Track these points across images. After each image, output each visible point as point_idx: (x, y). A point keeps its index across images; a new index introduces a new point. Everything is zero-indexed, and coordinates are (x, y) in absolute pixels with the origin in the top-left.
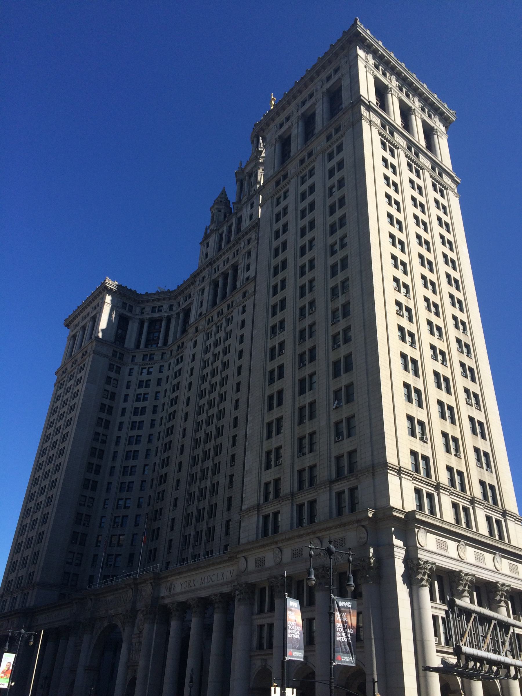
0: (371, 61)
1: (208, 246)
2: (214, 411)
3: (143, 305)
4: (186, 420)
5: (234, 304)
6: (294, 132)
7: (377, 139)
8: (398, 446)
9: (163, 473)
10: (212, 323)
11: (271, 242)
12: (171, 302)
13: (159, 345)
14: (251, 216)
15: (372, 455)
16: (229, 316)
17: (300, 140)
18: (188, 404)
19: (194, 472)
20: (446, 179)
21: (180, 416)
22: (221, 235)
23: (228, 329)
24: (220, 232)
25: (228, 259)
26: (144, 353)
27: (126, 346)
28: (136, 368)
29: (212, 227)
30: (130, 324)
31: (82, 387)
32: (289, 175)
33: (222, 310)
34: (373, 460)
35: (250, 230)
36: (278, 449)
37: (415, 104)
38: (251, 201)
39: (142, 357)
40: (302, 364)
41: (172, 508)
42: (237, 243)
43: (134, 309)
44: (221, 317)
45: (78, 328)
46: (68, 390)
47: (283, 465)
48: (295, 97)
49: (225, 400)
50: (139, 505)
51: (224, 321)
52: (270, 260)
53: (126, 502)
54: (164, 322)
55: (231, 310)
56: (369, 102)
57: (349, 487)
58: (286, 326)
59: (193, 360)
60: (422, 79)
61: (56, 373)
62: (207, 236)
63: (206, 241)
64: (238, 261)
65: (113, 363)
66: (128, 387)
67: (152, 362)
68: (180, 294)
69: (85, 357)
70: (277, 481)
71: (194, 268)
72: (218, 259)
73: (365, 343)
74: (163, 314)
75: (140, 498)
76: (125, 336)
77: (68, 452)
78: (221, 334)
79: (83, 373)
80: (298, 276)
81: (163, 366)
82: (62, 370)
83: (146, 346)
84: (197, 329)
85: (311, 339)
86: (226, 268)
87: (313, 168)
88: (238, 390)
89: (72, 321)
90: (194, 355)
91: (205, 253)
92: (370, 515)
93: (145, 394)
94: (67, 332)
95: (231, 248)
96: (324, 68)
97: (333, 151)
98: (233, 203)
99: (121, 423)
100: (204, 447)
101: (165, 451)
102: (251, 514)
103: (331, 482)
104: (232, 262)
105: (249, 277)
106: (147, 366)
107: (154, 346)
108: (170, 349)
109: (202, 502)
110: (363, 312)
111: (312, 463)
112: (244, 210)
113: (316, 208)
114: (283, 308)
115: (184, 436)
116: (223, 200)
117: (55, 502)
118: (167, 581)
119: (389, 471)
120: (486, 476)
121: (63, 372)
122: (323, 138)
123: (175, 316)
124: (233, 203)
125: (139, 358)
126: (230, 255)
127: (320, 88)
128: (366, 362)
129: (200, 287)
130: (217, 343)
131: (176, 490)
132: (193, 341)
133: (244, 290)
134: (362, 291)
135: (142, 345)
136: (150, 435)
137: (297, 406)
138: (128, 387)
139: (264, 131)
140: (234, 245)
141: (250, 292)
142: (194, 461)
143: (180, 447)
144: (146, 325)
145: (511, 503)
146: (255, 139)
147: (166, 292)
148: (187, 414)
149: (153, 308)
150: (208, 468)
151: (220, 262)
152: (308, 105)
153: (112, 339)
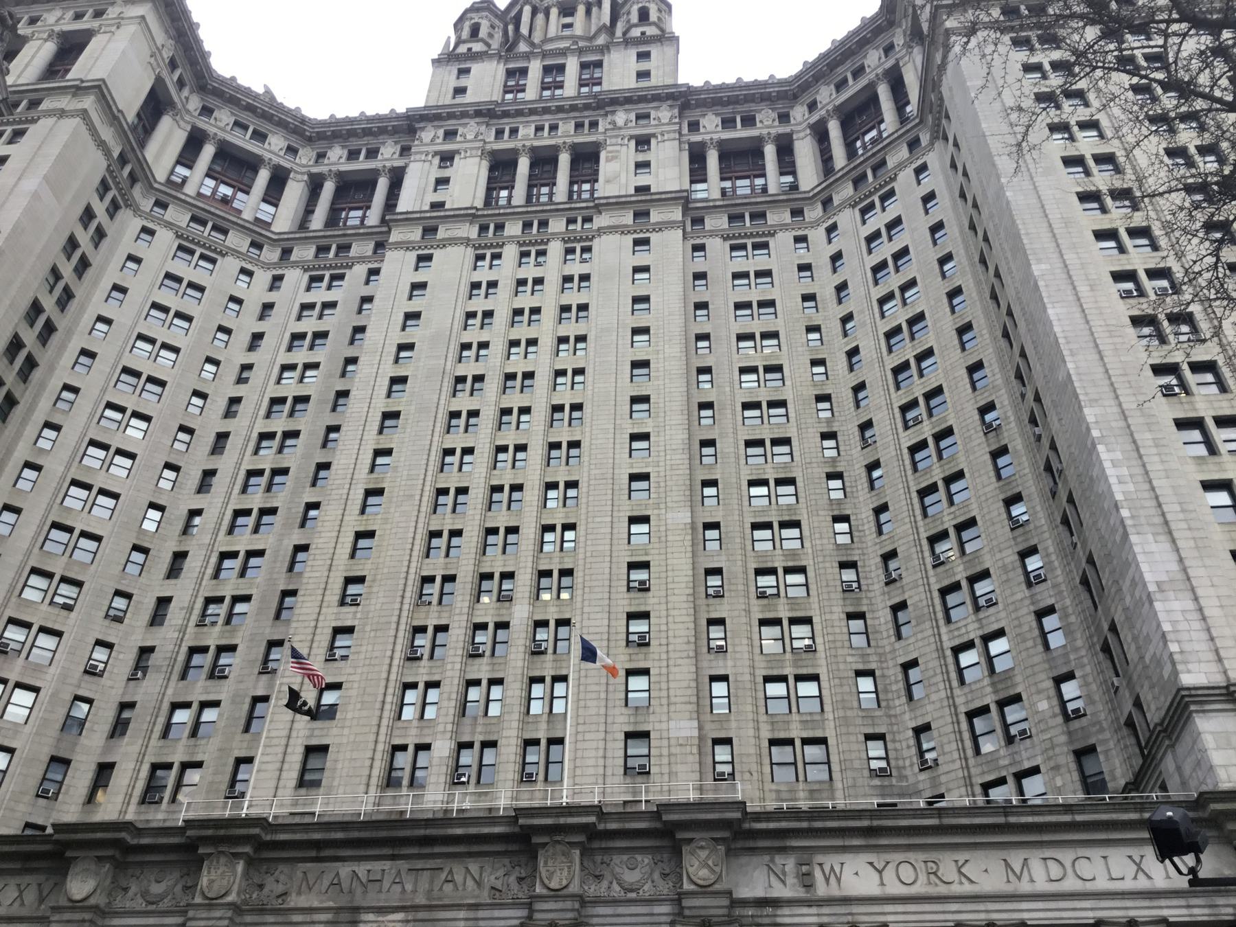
3: (212, 102)
24: (511, 66)
28: (165, 239)
30: (166, 122)
54: (263, 176)
91: (452, 82)
108: (287, 245)
109: (485, 660)
118: (783, 850)
123: (306, 177)
144: (208, 151)
153: (131, 116)
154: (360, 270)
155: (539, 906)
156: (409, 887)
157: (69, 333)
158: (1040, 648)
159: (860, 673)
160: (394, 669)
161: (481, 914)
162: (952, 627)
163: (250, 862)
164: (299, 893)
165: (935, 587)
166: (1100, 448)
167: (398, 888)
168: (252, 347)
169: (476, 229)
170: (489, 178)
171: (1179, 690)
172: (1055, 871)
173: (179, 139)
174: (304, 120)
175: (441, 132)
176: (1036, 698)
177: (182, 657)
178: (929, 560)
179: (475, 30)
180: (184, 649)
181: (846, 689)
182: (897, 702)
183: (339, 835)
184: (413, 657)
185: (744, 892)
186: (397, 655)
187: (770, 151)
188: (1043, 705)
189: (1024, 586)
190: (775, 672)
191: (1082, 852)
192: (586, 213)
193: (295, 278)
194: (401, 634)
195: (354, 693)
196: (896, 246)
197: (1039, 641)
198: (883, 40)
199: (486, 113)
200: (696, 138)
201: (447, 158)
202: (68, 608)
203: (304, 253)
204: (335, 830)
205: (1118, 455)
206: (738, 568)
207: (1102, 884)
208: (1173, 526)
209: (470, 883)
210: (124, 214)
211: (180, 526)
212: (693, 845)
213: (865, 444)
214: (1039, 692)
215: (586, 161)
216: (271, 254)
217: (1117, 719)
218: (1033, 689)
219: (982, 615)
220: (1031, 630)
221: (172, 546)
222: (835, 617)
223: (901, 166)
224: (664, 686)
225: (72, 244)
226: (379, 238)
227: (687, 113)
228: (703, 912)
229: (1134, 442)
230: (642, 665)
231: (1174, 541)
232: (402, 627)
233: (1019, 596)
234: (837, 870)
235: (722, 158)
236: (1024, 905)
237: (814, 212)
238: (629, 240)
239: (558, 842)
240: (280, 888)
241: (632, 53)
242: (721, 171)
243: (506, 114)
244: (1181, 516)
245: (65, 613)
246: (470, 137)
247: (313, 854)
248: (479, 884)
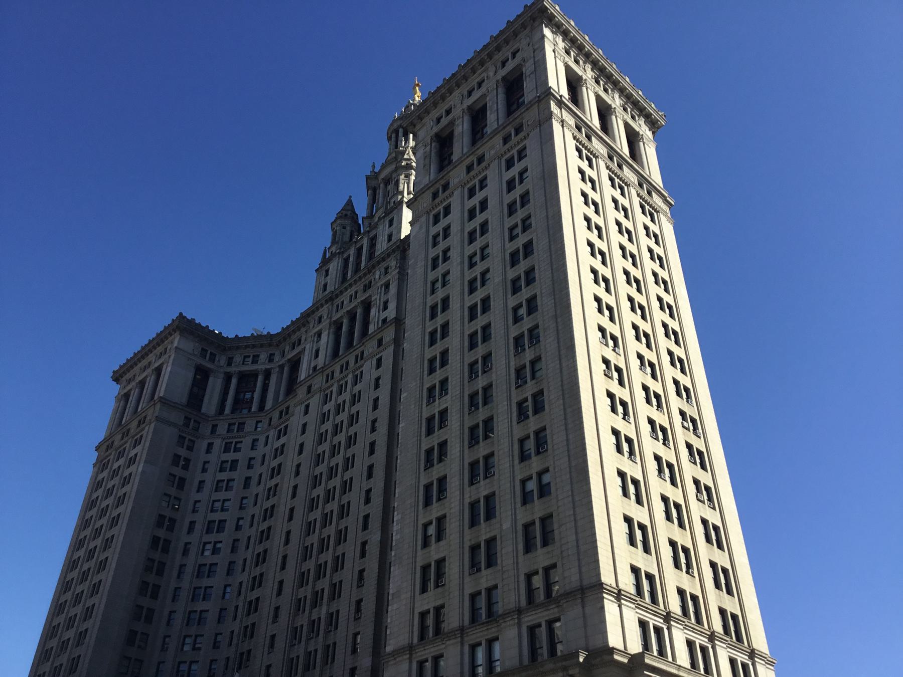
0: (561, 45)
1: (327, 275)
2: (334, 506)
4: (290, 518)
5: (365, 355)
6: (458, 130)
7: (571, 144)
8: (616, 560)
9: (253, 598)
10: (333, 381)
11: (426, 273)
13: (254, 409)
14: (390, 237)
15: (580, 572)
16: (358, 372)
17: (467, 140)
18: (294, 495)
19: (301, 595)
20: (657, 200)
21: (282, 511)
22: (346, 261)
23: (357, 389)
24: (345, 256)
25: (356, 293)
26: (232, 421)
27: (203, 410)
28: (218, 444)
29: (333, 249)
30: (211, 380)
31: (138, 469)
32: (451, 185)
33: (347, 363)
34: (581, 580)
35: (389, 255)
36: (440, 563)
37: (615, 101)
38: (391, 216)
39: (227, 426)
40: (473, 441)
41: (266, 649)
42: (370, 272)
43: (217, 359)
44: (345, 373)
45: (133, 384)
46: (115, 473)
47: (447, 587)
48: (458, 85)
49: (350, 490)
50: (216, 646)
51: (350, 378)
52: (425, 296)
53: (195, 640)
54: (260, 378)
55: (360, 363)
56: (561, 96)
57: (547, 618)
58: (450, 387)
59: (303, 432)
60: (623, 71)
61: (97, 449)
62: (325, 261)
63: (325, 268)
64: (370, 296)
65: (184, 435)
66: (204, 470)
67: (241, 434)
68: (285, 339)
69: (142, 426)
70: (438, 610)
71: (307, 303)
72: (341, 292)
73: (565, 414)
74: (262, 366)
75: (217, 635)
76: (203, 396)
77: (112, 565)
78: (346, 396)
79: (138, 449)
80: (466, 320)
81: (258, 440)
82: (106, 444)
83: (233, 411)
84: (310, 388)
85: (486, 407)
86: (353, 306)
87: (485, 178)
88: (370, 476)
89: (124, 373)
90: (305, 425)
92: (581, 660)
93: (229, 481)
94: (115, 389)
95: (360, 278)
96: (498, 49)
97: (513, 157)
98: (363, 218)
99: (192, 523)
100: (317, 559)
101: (257, 565)
102: (401, 658)
103: (519, 611)
104: (362, 297)
105: (386, 319)
107: (245, 411)
108: (269, 416)
109: (312, 641)
110: (561, 372)
111: (490, 584)
112: (380, 228)
113: (490, 229)
114: (444, 363)
115: (287, 542)
116: (348, 213)
117: (91, 639)
119: (605, 595)
120: (727, 601)
121: (108, 448)
122: (498, 140)
123: (277, 369)
124: (363, 218)
125: (222, 429)
126: (359, 287)
127: (493, 75)
128: (567, 440)
129: (316, 330)
130: (339, 409)
131: (274, 622)
132: (303, 406)
133: (379, 336)
134: (558, 343)
135: (227, 410)
136: (235, 541)
137: (467, 501)
138: (204, 470)
139: (415, 126)
140: (365, 275)
141: (388, 339)
142: (303, 579)
143: (280, 558)
144: (234, 381)
145: (759, 640)
146: (394, 135)
147: (265, 336)
148: (292, 510)
149: (245, 357)
150: (323, 590)
151: (345, 298)
152: (476, 95)
153: (184, 400)
192: (361, 349)
201: (319, 335)
211: (236, 594)
230: (358, 630)
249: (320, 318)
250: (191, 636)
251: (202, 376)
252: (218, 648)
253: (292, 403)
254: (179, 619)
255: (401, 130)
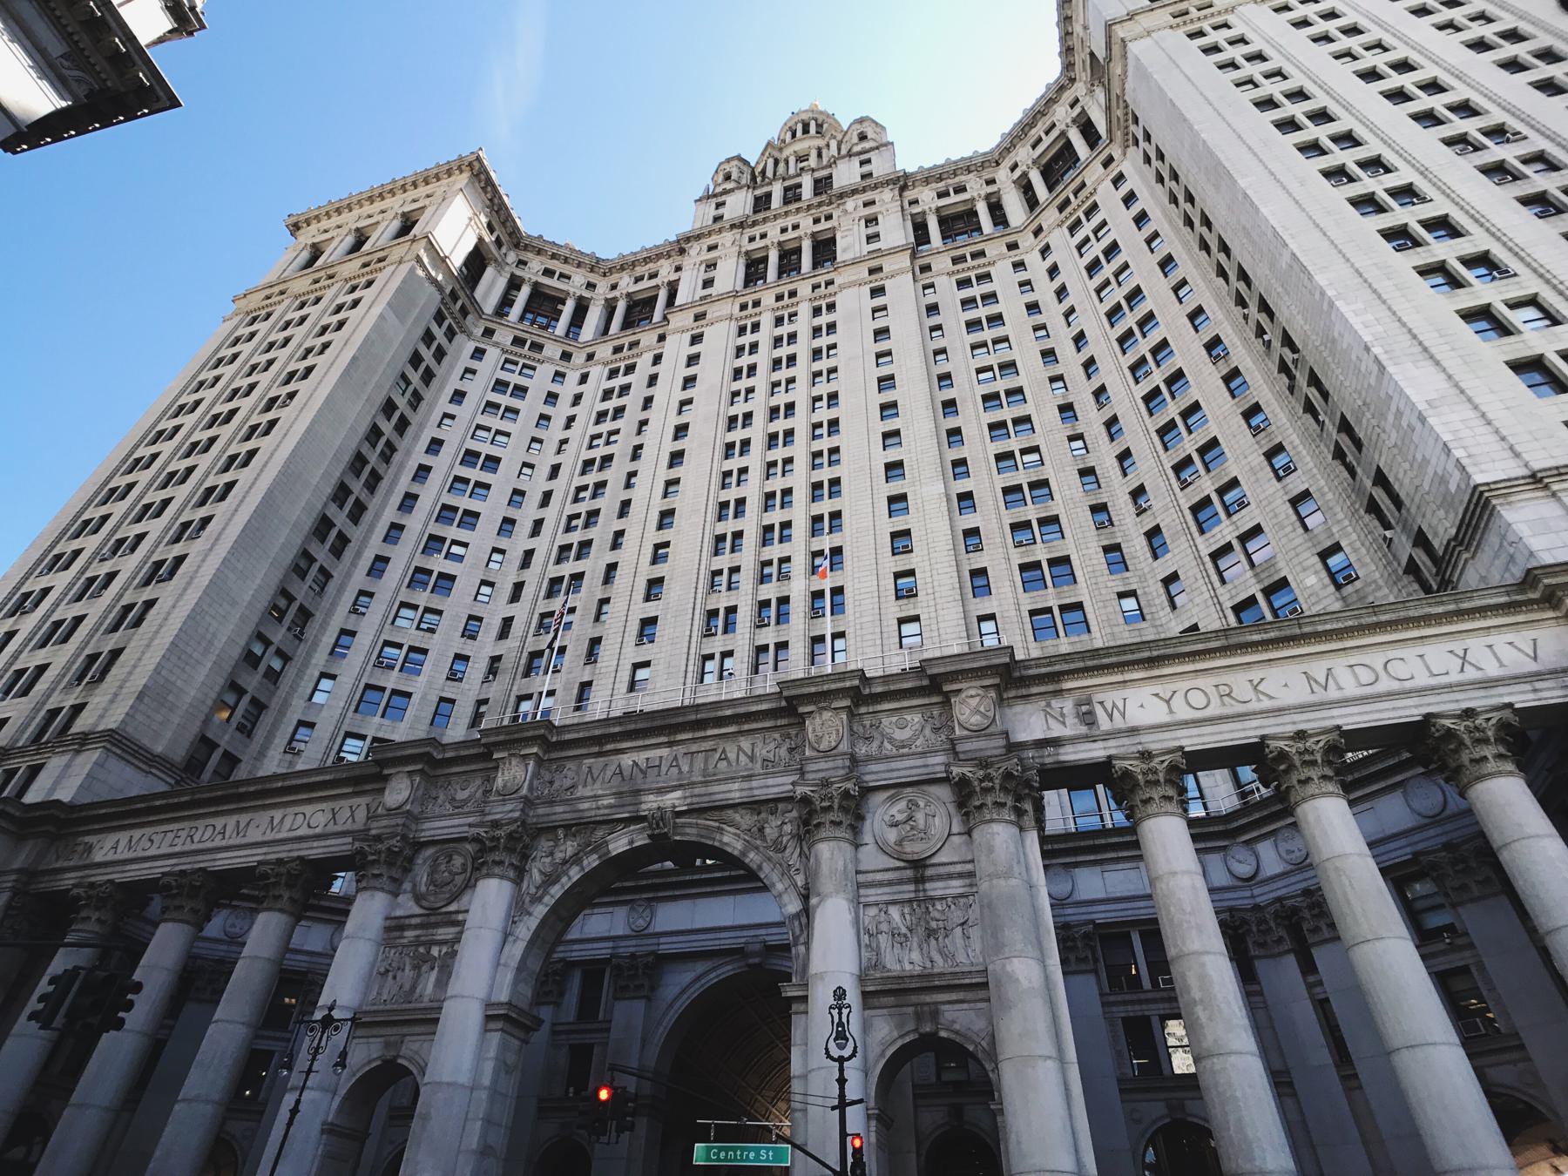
12: (593, 278)
24: (758, 192)
30: (490, 272)
42: (831, 203)
63: (714, 201)
67: (537, 356)
82: (267, 292)
91: (712, 212)
106: (522, 361)
108: (590, 350)
125: (504, 336)
131: (647, 599)
144: (525, 291)
146: (799, 128)
154: (648, 357)
155: (811, 767)
156: (685, 768)
157: (422, 426)
158: (1301, 530)
159: (1121, 595)
160: (693, 645)
161: (754, 784)
162: (1207, 535)
163: (540, 762)
164: (585, 785)
165: (1185, 506)
166: (1338, 303)
167: (675, 770)
168: (568, 427)
169: (737, 307)
170: (747, 275)
171: (1476, 487)
172: (1365, 675)
173: (502, 283)
174: (598, 260)
175: (705, 248)
176: (1302, 576)
177: (523, 661)
178: (1176, 485)
179: (728, 177)
180: (525, 654)
181: (1110, 609)
182: (1161, 614)
183: (617, 729)
184: (708, 633)
185: (1022, 736)
186: (695, 634)
187: (982, 209)
188: (1311, 580)
189: (1274, 481)
190: (1039, 606)
191: (1392, 654)
193: (597, 373)
194: (697, 617)
195: (661, 667)
196: (1105, 242)
197: (1298, 524)
198: (1068, 96)
199: (740, 225)
200: (916, 209)
202: (432, 631)
203: (604, 351)
204: (614, 725)
205: (1360, 305)
206: (994, 525)
207: (1423, 680)
208: (1433, 350)
209: (743, 758)
210: (459, 338)
211: (517, 563)
212: (963, 695)
213: (1101, 406)
214: (1305, 570)
215: (825, 249)
216: (579, 358)
217: (1395, 571)
218: (1299, 568)
219: (1235, 518)
220: (1288, 517)
221: (513, 578)
222: (1092, 551)
223: (1100, 181)
224: (934, 627)
225: (416, 360)
226: (660, 331)
227: (906, 193)
228: (978, 755)
229: (1375, 291)
230: (912, 613)
231: (1437, 363)
232: (697, 611)
233: (1271, 491)
234: (1120, 704)
235: (943, 222)
236: (1335, 712)
237: (1027, 241)
238: (866, 290)
239: (824, 709)
240: (568, 783)
241: (856, 161)
242: (942, 232)
243: (754, 224)
244: (1441, 341)
245: (428, 635)
246: (728, 244)
247: (596, 749)
248: (752, 758)
249: (711, 248)
250: (415, 607)
251: (477, 261)
252: (473, 638)
253: (648, 338)
254: (395, 572)
255: (813, 124)
